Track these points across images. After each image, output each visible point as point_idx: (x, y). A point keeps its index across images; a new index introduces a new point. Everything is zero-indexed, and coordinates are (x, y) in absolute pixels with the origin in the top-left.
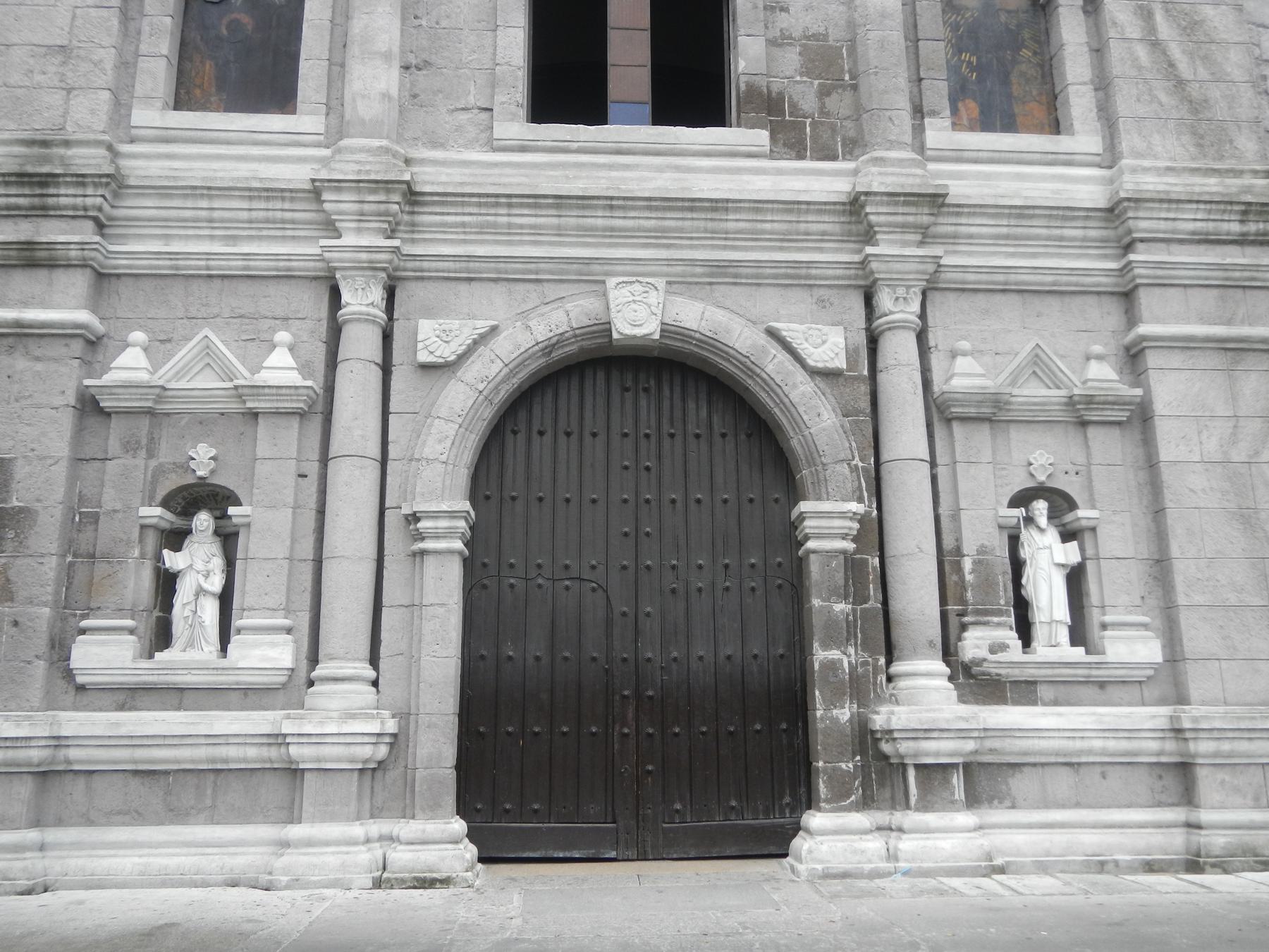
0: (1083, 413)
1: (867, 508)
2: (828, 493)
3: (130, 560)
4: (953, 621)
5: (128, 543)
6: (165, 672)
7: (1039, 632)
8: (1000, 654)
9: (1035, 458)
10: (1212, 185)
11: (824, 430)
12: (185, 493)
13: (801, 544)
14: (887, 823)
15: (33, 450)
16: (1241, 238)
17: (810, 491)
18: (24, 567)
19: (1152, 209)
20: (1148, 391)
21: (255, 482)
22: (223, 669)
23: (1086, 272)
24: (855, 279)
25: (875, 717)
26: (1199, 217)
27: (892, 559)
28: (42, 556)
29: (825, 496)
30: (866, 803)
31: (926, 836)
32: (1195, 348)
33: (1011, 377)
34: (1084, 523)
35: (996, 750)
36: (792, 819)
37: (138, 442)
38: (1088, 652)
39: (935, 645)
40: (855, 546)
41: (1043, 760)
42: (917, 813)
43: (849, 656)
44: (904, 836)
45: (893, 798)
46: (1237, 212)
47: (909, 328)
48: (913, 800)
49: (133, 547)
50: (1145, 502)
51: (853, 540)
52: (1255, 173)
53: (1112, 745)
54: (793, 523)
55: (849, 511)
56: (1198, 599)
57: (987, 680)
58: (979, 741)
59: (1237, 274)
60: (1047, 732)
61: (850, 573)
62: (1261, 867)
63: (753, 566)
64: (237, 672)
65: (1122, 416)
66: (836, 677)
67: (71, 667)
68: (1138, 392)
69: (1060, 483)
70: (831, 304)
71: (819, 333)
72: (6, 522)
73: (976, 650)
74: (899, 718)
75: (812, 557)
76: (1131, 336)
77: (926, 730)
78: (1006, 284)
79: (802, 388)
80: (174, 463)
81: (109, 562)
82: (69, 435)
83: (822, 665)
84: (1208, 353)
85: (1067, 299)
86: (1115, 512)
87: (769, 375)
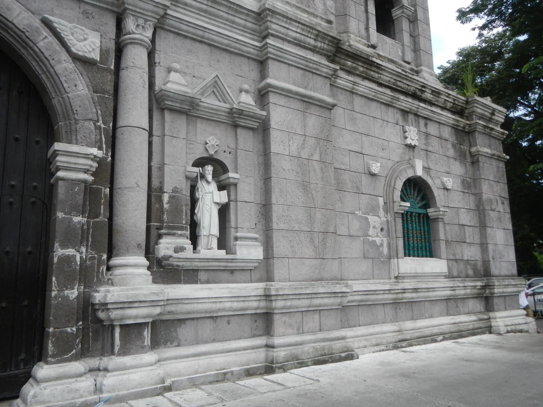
0: (236, 119)
1: (104, 155)
2: (77, 140)
4: (154, 232)
7: (202, 241)
8: (180, 253)
9: (209, 140)
10: (304, 17)
11: (79, 96)
13: (53, 174)
14: (97, 366)
16: (314, 48)
17: (64, 136)
19: (279, 19)
20: (269, 114)
23: (245, 44)
24: (111, 6)
25: (96, 294)
26: (298, 31)
27: (118, 190)
29: (75, 142)
30: (82, 354)
31: (123, 372)
32: (290, 97)
33: (201, 90)
34: (232, 180)
35: (172, 312)
36: (26, 370)
38: (227, 253)
39: (141, 246)
40: (93, 178)
41: (198, 316)
42: (118, 357)
43: (82, 253)
44: (108, 374)
45: (103, 348)
46: (314, 34)
47: (144, 46)
48: (117, 349)
50: (261, 173)
51: (92, 175)
52: (322, 18)
53: (235, 305)
54: (49, 160)
55: (91, 154)
56: (282, 226)
57: (171, 269)
58: (163, 307)
59: (311, 65)
60: (202, 299)
61: (87, 197)
62: (300, 365)
63: (12, 186)
65: (255, 125)
66: (70, 267)
68: (264, 113)
69: (221, 157)
70: (93, 17)
71: (82, 32)
73: (166, 251)
74: (113, 295)
75: (61, 183)
76: (263, 83)
77: (130, 302)
78: (203, 37)
79: (65, 65)
83: (60, 258)
84: (296, 101)
85: (233, 57)
86: (247, 177)
87: (40, 49)
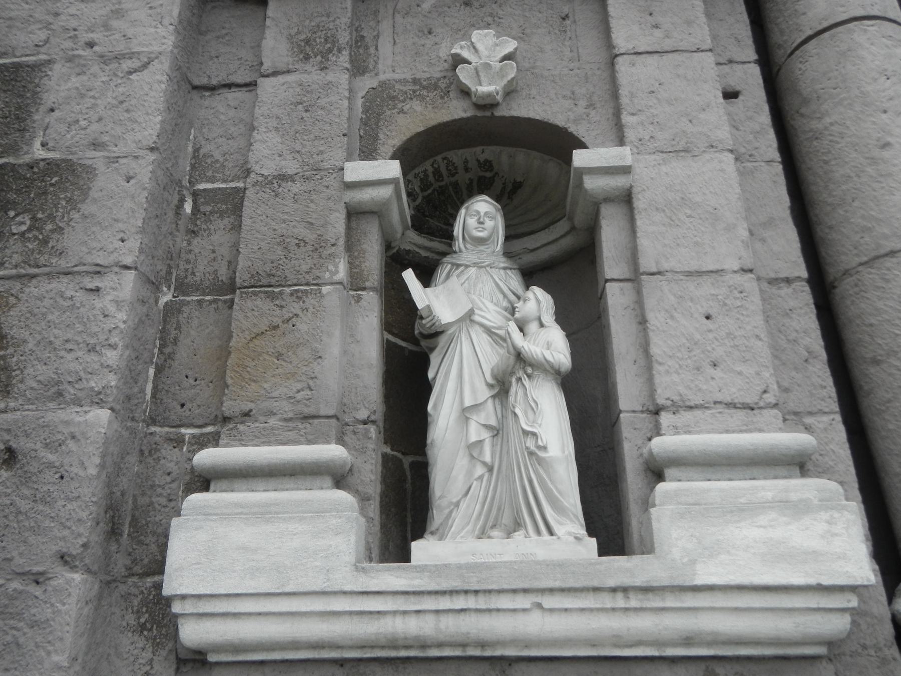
3: (325, 289)
5: (319, 247)
6: (460, 603)
12: (427, 166)
15: (91, 45)
18: (47, 302)
21: (624, 100)
22: (646, 590)
28: (99, 271)
37: (331, 39)
49: (332, 256)
64: (690, 600)
67: (167, 591)
72: (12, 196)
80: (415, 81)
81: (272, 296)
82: (176, 12)
